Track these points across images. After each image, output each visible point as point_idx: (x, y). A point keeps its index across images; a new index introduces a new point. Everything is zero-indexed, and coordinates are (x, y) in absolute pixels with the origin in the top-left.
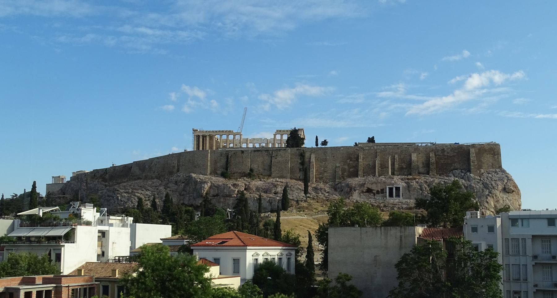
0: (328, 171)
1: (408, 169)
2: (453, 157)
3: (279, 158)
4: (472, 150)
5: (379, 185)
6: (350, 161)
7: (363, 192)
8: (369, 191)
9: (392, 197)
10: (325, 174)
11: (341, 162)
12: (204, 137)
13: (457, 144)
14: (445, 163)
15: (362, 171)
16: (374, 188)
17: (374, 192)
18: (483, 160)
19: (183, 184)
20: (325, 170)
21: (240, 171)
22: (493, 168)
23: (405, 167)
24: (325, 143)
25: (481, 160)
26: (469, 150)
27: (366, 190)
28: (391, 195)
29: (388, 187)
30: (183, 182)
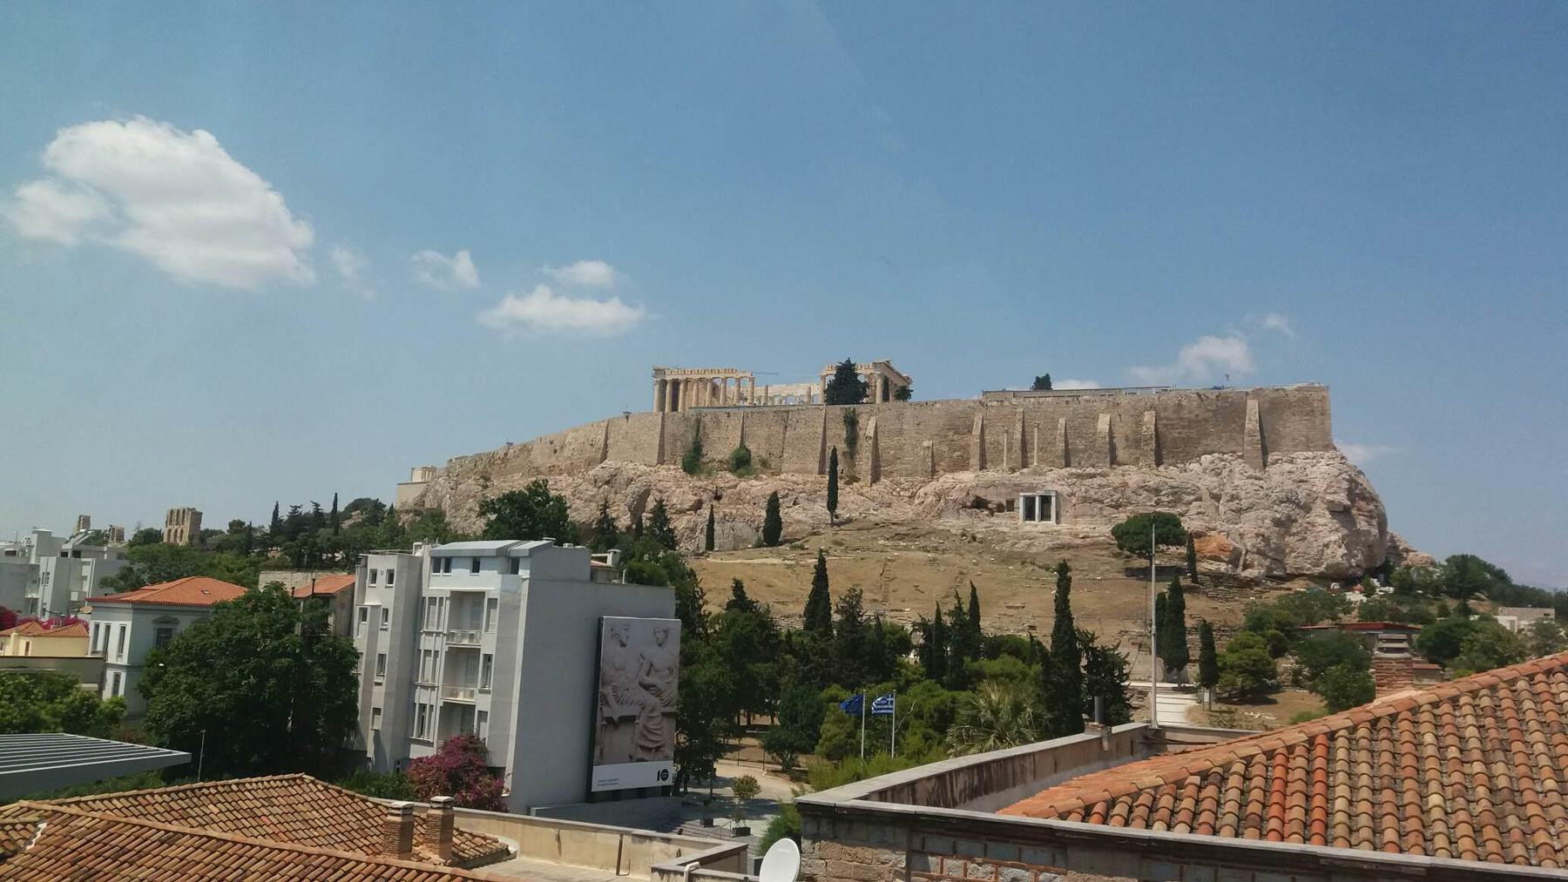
0: (903, 457)
1: (1090, 451)
2: (1204, 423)
3: (801, 430)
4: (1253, 406)
5: (1003, 490)
6: (956, 433)
7: (965, 506)
8: (980, 504)
9: (1034, 520)
10: (899, 467)
11: (935, 438)
12: (676, 383)
13: (1219, 388)
14: (1183, 438)
15: (978, 457)
16: (994, 498)
17: (990, 506)
18: (1281, 429)
19: (606, 487)
20: (898, 456)
21: (719, 457)
22: (1308, 449)
23: (1083, 447)
24: (904, 394)
25: (1278, 430)
26: (1246, 403)
27: (974, 501)
28: (1029, 515)
29: (1022, 494)
30: (607, 483)
